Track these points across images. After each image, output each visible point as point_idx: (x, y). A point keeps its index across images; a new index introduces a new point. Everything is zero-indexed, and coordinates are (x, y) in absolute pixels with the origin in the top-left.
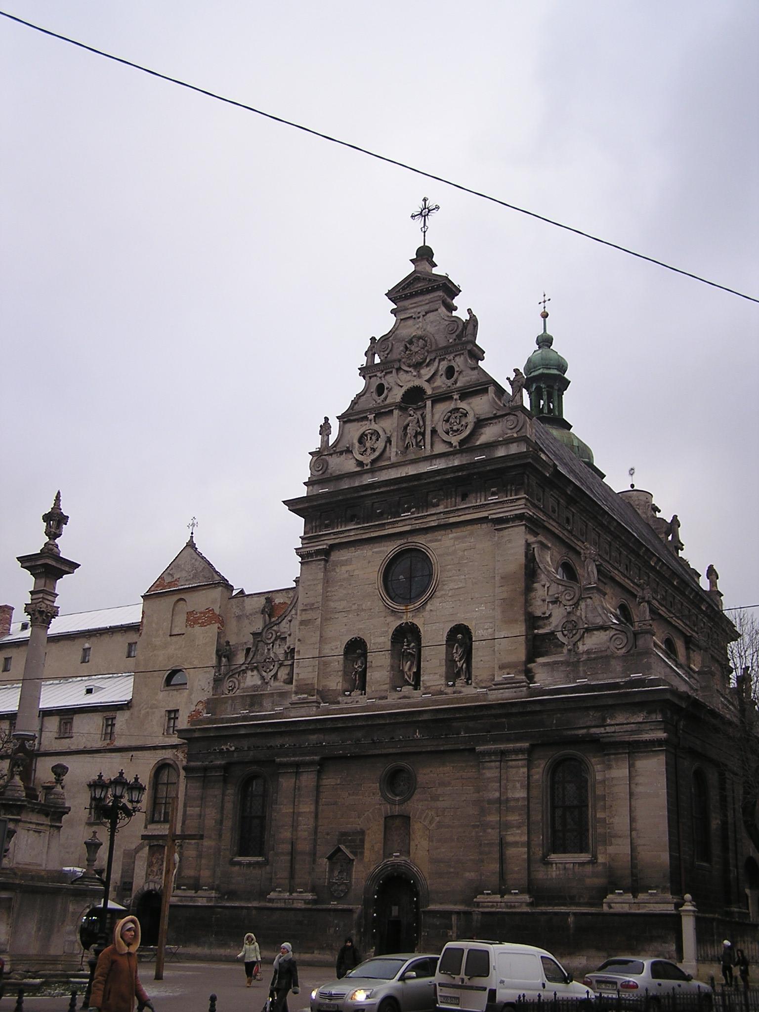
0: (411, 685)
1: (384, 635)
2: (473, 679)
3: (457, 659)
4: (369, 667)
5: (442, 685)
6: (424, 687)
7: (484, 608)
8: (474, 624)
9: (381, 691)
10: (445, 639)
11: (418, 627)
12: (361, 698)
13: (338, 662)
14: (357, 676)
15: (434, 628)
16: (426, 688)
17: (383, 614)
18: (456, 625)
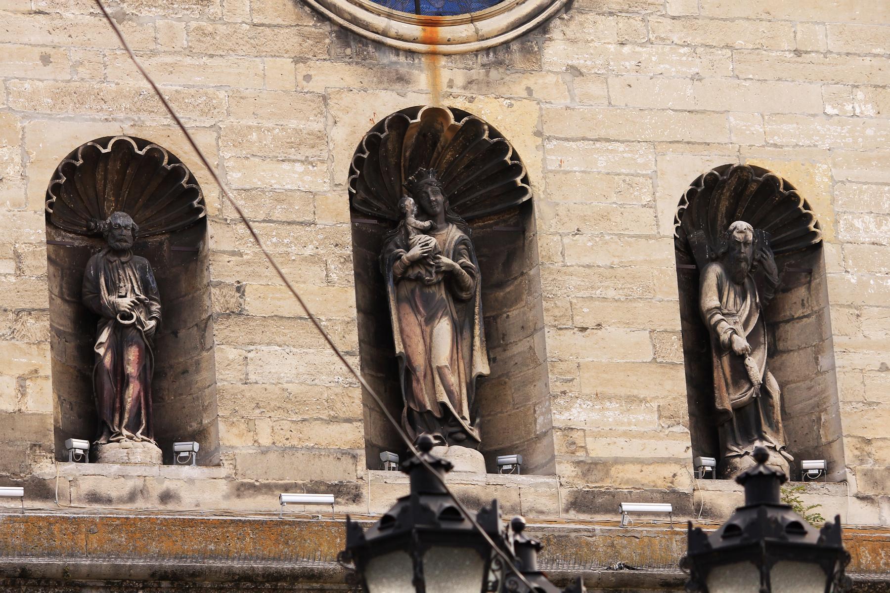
0: (468, 441)
1: (310, 152)
2: (849, 453)
3: (741, 343)
4: (229, 314)
5: (677, 461)
6: (578, 463)
7: (870, 110)
8: (821, 178)
9: (315, 451)
10: (669, 229)
11: (502, 146)
12: (191, 481)
13: (18, 257)
14: (132, 354)
15: (602, 163)
16: (589, 467)
17: (289, 40)
18: (723, 169)
